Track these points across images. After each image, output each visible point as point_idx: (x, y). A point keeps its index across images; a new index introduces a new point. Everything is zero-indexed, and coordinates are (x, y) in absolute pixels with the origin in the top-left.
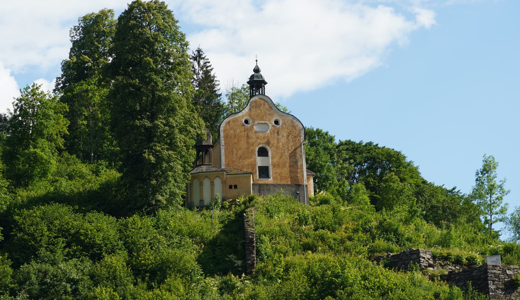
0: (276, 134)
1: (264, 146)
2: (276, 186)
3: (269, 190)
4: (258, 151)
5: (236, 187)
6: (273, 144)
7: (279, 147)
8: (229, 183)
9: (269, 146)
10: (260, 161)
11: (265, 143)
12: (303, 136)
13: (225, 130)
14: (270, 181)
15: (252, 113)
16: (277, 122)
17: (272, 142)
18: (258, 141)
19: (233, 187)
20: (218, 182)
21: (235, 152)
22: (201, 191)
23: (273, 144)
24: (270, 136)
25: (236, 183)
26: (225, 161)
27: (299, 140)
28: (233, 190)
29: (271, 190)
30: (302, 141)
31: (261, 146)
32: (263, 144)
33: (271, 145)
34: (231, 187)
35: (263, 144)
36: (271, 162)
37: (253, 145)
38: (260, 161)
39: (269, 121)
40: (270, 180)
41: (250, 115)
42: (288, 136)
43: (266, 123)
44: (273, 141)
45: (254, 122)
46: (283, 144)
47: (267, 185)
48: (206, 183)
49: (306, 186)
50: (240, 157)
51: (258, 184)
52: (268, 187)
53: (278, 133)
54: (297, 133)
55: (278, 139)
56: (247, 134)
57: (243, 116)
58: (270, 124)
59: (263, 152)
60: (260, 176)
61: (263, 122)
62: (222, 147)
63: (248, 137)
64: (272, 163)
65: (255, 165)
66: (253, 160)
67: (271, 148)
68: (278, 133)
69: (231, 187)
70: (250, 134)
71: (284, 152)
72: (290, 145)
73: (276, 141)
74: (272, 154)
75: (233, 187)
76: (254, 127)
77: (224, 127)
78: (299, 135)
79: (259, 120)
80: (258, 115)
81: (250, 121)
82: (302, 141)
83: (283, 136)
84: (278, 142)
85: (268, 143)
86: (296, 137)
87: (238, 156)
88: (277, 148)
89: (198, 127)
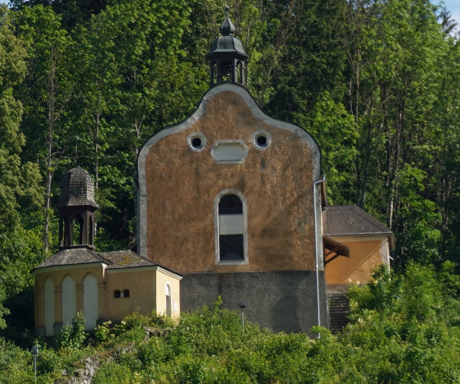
0: (259, 166)
1: (233, 191)
2: (256, 277)
3: (240, 286)
4: (220, 204)
5: (127, 294)
6: (252, 187)
7: (266, 192)
8: (113, 287)
9: (243, 191)
10: (224, 225)
11: (235, 187)
12: (316, 166)
13: (149, 163)
14: (244, 265)
15: (209, 125)
16: (262, 141)
17: (249, 184)
18: (221, 182)
19: (122, 295)
20: (91, 285)
21: (169, 209)
22: (58, 305)
23: (252, 187)
24: (245, 170)
25: (128, 287)
26: (148, 229)
27: (309, 177)
28: (122, 300)
29: (246, 285)
30: (314, 177)
31: (225, 192)
32: (230, 187)
33: (247, 190)
34: (117, 294)
35: (230, 187)
36: (246, 225)
37: (208, 191)
38: (224, 225)
39: (243, 138)
40: (242, 263)
41: (203, 129)
42: (285, 169)
43: (239, 144)
44: (253, 182)
45: (211, 142)
46: (273, 187)
47: (237, 275)
48: (69, 285)
49: (321, 273)
50: (181, 218)
51: (215, 275)
52: (238, 280)
53: (263, 165)
54: (305, 160)
55: (263, 175)
56: (197, 169)
57: (188, 131)
58: (245, 146)
59: (231, 205)
60: (223, 257)
61: (231, 141)
62: (142, 198)
63: (198, 174)
64: (249, 227)
65: (212, 234)
66: (207, 222)
67: (247, 195)
68: (263, 165)
69: (117, 294)
70: (203, 168)
71: (276, 204)
72: (288, 189)
73: (257, 181)
74: (249, 209)
75: (122, 295)
76: (212, 152)
77: (147, 157)
78: (308, 168)
79: (222, 138)
80: (220, 128)
81: (204, 141)
82: (314, 177)
83: (274, 169)
84: (263, 182)
85: (241, 186)
86: (301, 170)
87: (176, 216)
88: (262, 194)
89: (21, 182)
